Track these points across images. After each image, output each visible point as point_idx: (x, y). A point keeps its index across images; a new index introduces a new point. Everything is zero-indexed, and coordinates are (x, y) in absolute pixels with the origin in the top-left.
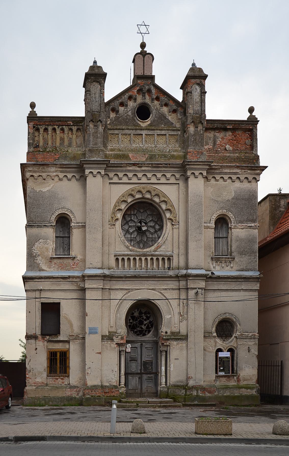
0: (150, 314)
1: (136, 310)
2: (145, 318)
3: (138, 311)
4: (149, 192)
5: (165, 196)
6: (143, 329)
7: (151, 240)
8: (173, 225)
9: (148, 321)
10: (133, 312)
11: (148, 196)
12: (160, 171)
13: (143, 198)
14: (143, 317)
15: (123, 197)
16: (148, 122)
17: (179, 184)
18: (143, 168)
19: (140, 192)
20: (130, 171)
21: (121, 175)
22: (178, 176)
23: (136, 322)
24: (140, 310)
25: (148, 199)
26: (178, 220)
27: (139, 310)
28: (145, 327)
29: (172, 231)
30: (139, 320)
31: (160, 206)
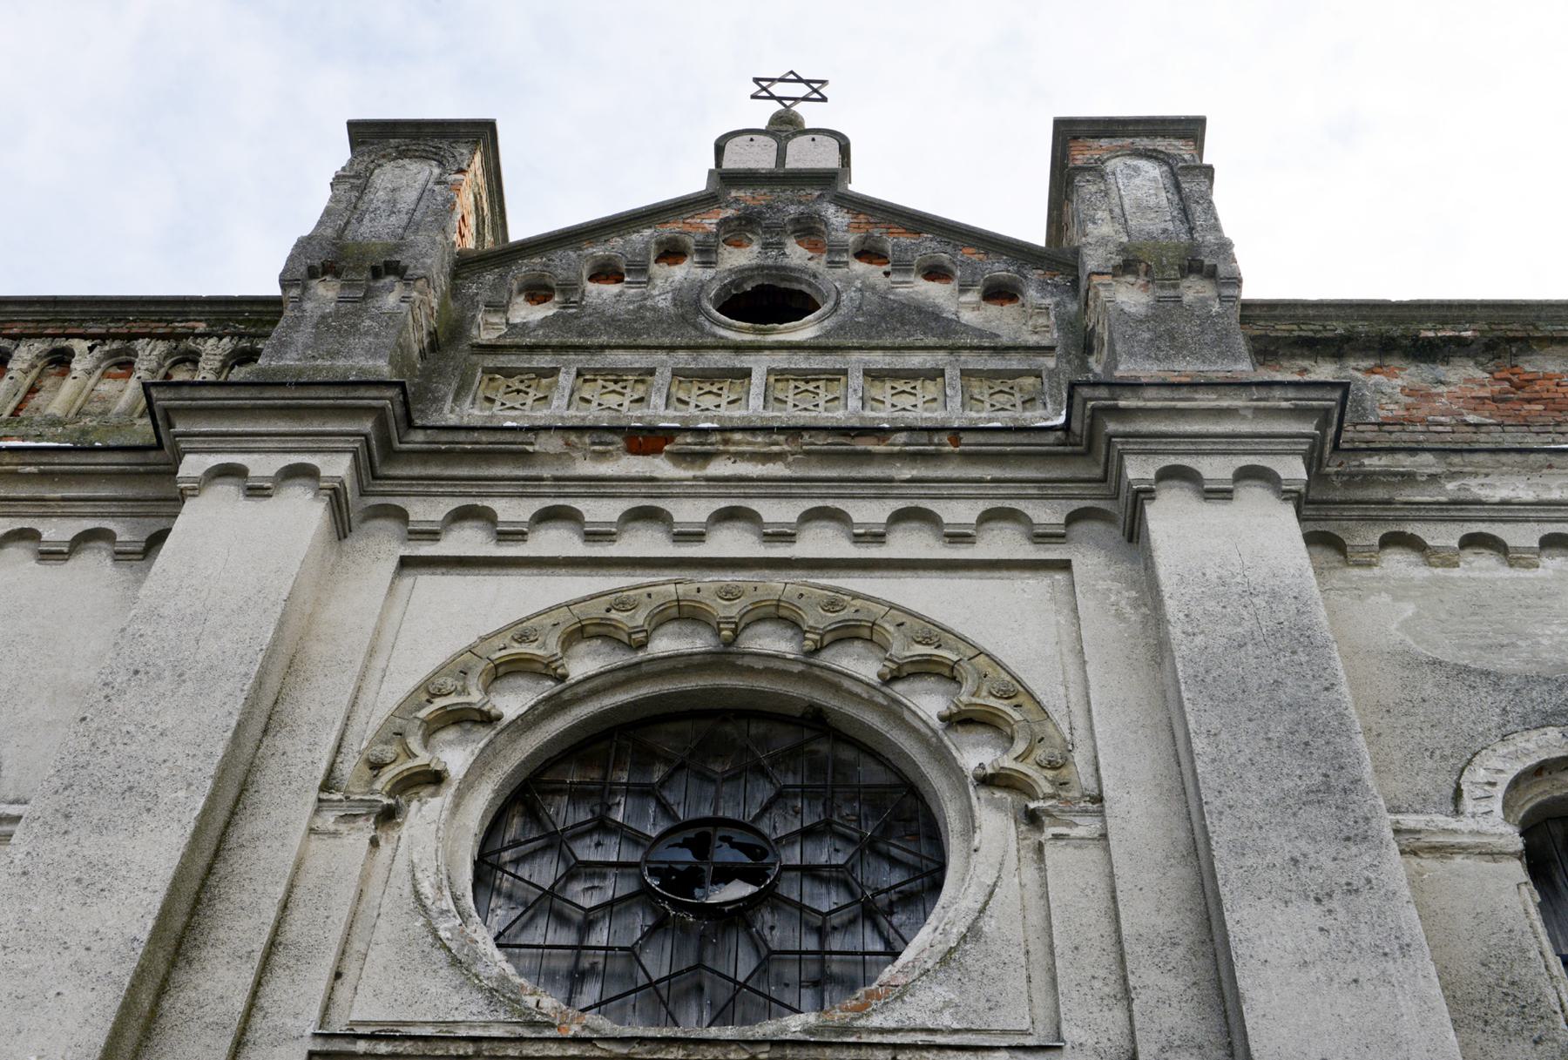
4: (780, 615)
5: (933, 633)
7: (812, 970)
8: (1033, 819)
11: (771, 642)
12: (881, 488)
13: (724, 658)
15: (523, 638)
16: (804, 330)
17: (1065, 566)
18: (719, 468)
19: (686, 614)
20: (599, 487)
21: (512, 511)
22: (1046, 514)
25: (773, 666)
26: (1087, 781)
29: (1030, 874)
31: (895, 712)
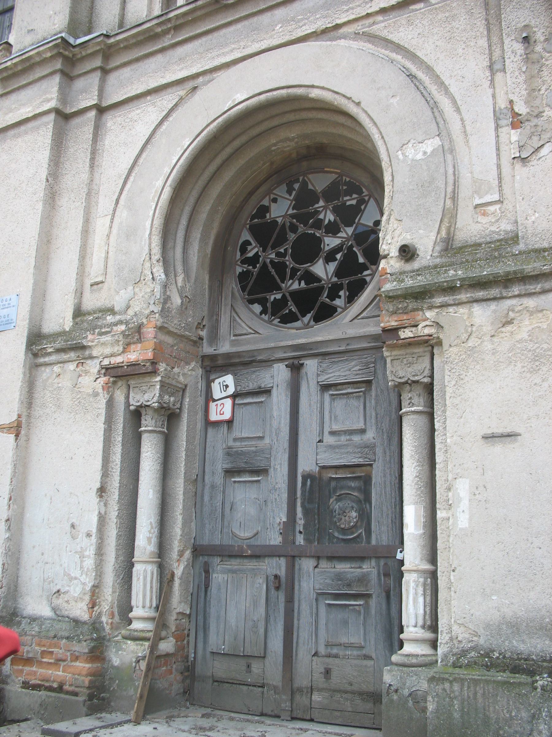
0: (360, 192)
1: (282, 191)
2: (330, 217)
3: (289, 192)
6: (319, 280)
9: (350, 230)
10: (266, 202)
14: (321, 216)
23: (278, 254)
24: (304, 184)
27: (296, 186)
28: (332, 267)
30: (292, 237)
